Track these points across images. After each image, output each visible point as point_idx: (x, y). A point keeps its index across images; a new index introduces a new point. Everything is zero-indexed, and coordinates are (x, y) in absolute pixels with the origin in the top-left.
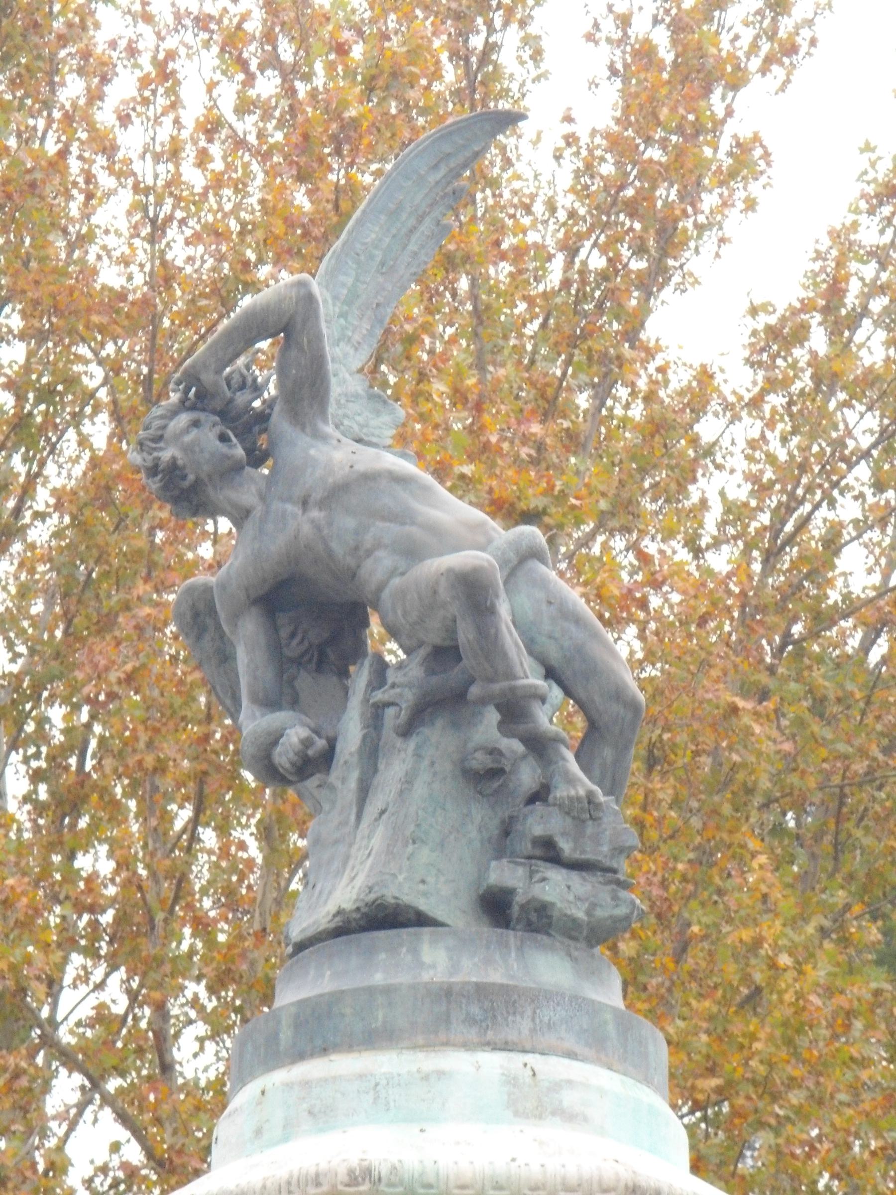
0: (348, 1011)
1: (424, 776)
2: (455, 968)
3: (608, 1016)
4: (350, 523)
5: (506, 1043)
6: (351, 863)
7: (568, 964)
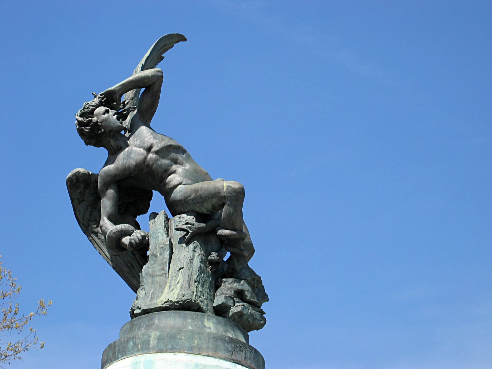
0: (183, 338)
5: (238, 361)
6: (168, 285)
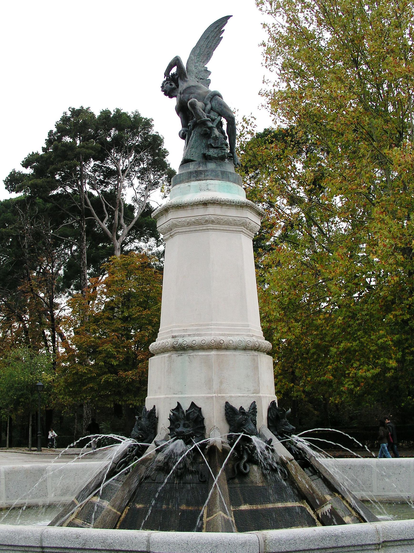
1: (194, 137)
2: (194, 168)
3: (220, 172)
4: (187, 95)
7: (215, 164)
